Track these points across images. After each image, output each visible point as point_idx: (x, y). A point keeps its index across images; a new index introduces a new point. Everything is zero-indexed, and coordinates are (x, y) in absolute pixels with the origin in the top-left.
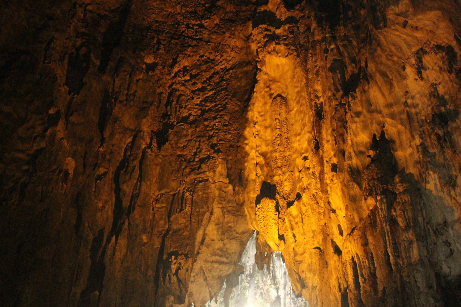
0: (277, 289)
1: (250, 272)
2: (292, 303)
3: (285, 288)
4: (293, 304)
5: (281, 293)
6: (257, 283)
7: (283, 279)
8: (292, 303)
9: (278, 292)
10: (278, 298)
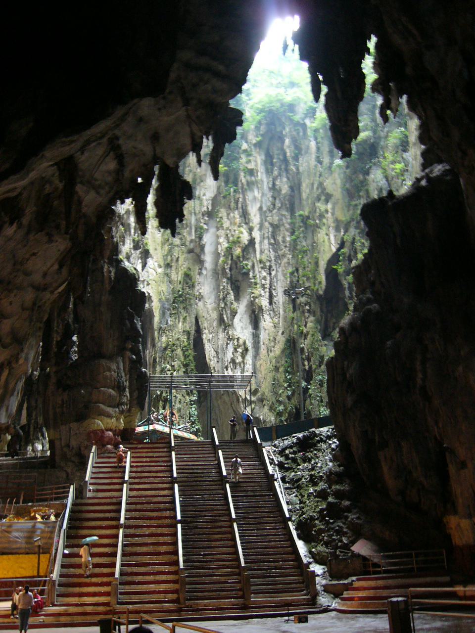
0: (251, 230)
1: (208, 208)
2: (271, 250)
3: (260, 229)
4: (274, 251)
5: (256, 234)
6: (220, 221)
7: (258, 216)
8: (271, 250)
9: (250, 234)
10: (252, 242)
